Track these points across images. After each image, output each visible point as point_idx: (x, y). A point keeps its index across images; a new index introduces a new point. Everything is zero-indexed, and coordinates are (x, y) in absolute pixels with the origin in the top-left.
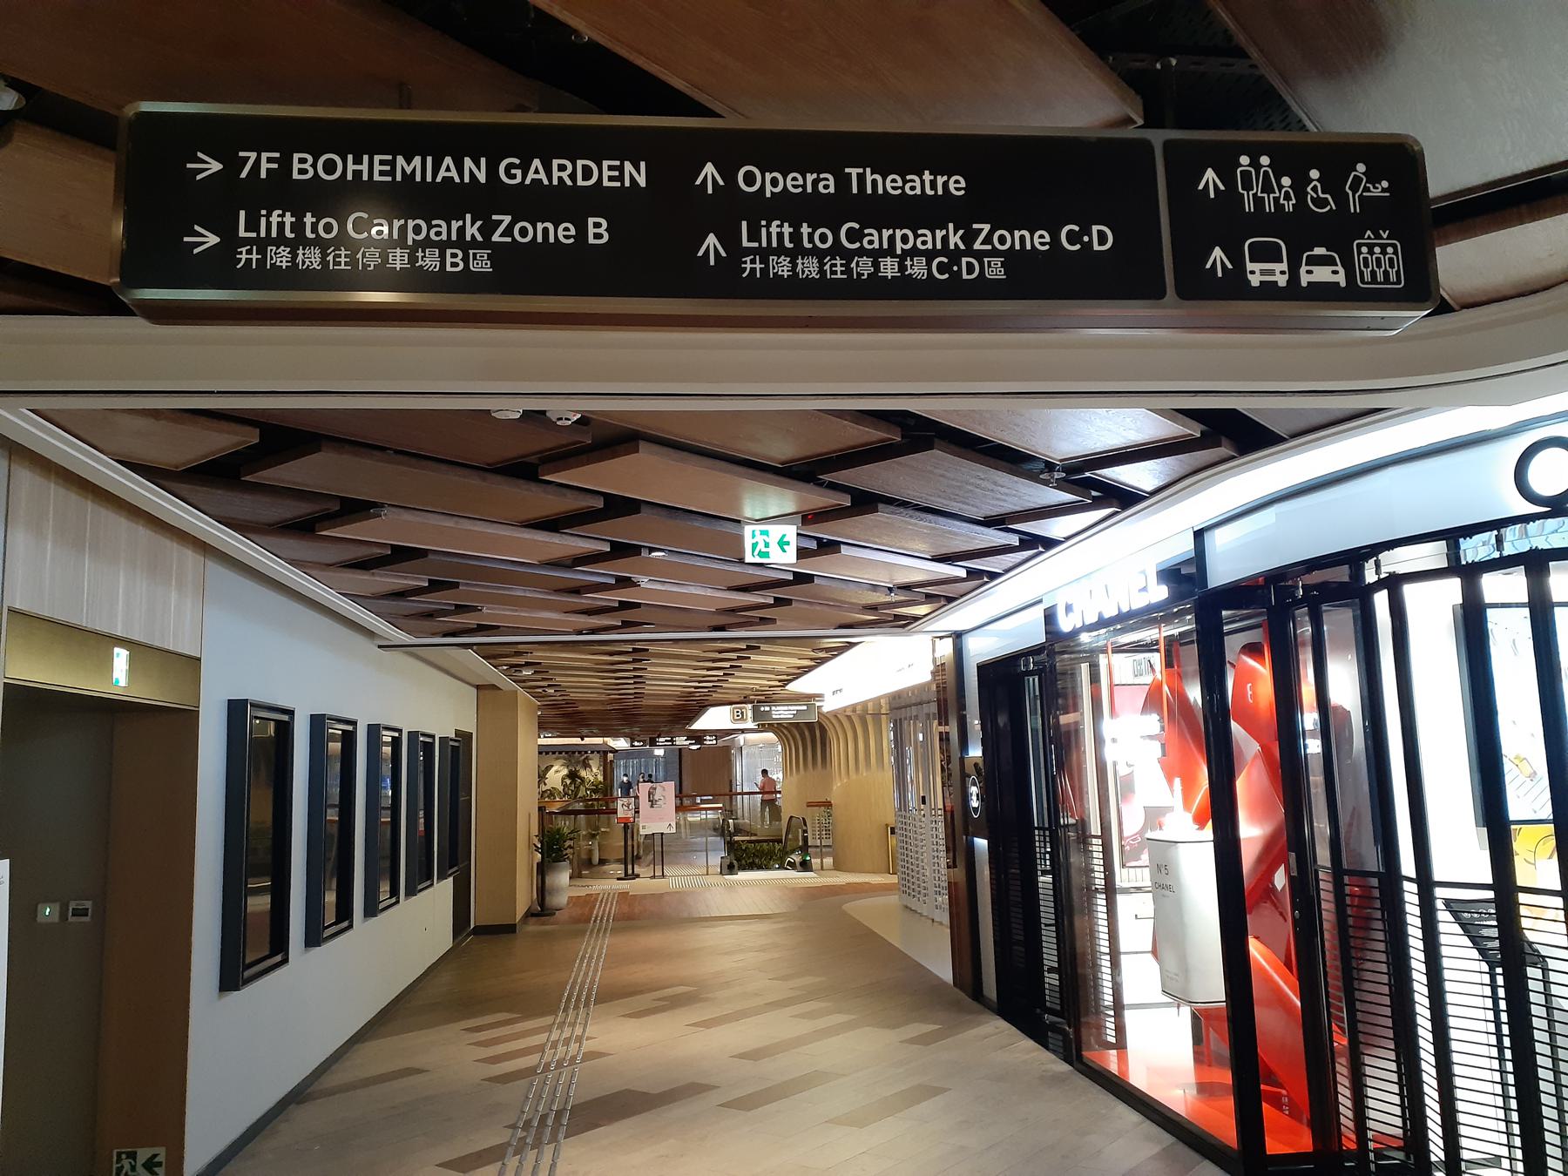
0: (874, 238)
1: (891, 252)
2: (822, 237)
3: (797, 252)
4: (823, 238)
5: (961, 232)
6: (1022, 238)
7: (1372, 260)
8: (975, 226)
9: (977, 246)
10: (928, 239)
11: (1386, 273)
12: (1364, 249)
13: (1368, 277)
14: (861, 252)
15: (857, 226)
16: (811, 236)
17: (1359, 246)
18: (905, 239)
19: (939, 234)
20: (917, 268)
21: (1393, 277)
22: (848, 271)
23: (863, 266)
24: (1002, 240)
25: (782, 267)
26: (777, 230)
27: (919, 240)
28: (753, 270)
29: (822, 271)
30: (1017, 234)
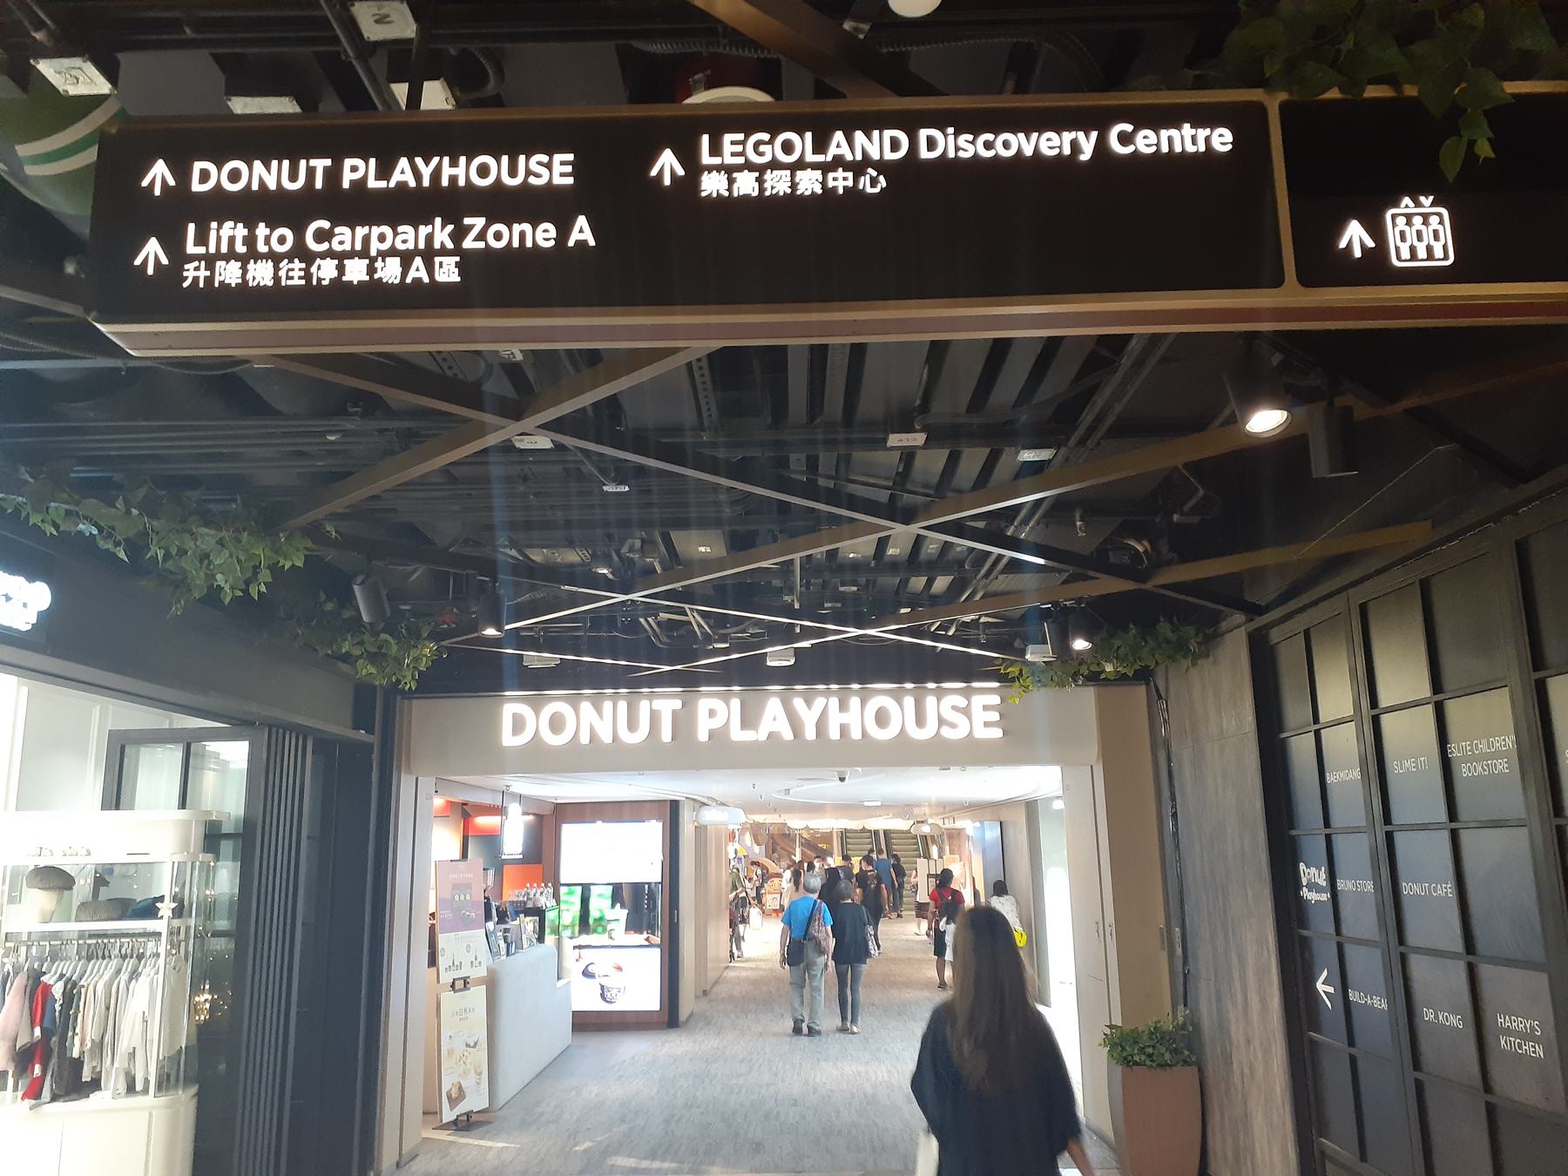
0: (344, 237)
2: (281, 238)
3: (253, 255)
4: (282, 240)
5: (450, 227)
6: (522, 235)
7: (1411, 236)
8: (467, 221)
9: (469, 243)
10: (408, 236)
11: (1429, 249)
13: (1406, 254)
15: (326, 224)
16: (267, 240)
17: (1394, 217)
18: (382, 238)
19: (424, 230)
21: (1439, 253)
23: (326, 271)
24: (498, 236)
25: (229, 273)
26: (232, 231)
27: (399, 238)
28: (196, 279)
29: (276, 278)
30: (517, 228)
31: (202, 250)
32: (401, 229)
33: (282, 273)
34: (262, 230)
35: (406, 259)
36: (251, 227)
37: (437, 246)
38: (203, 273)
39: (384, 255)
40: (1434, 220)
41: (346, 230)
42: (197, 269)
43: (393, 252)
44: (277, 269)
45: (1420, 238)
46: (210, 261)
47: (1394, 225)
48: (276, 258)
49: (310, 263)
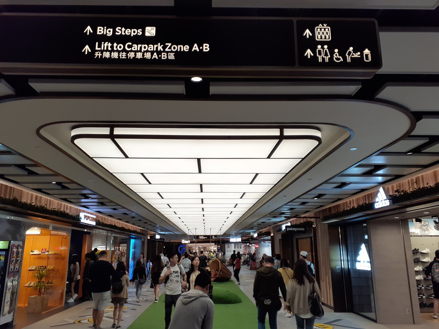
0: (135, 47)
1: (140, 51)
3: (112, 50)
4: (120, 47)
5: (162, 46)
6: (180, 48)
8: (167, 44)
10: (152, 47)
11: (325, 36)
12: (319, 29)
13: (319, 37)
14: (131, 51)
15: (130, 44)
17: (317, 29)
18: (145, 48)
19: (155, 46)
20: (148, 56)
22: (127, 56)
23: (131, 55)
24: (174, 48)
25: (107, 55)
26: (107, 45)
27: (149, 48)
28: (98, 56)
29: (119, 56)
30: (179, 46)
31: (100, 49)
32: (150, 45)
33: (120, 55)
34: (115, 45)
35: (152, 53)
36: (113, 44)
37: (159, 50)
38: (100, 55)
39: (144, 52)
40: (327, 30)
41: (136, 45)
42: (98, 53)
43: (147, 51)
44: (119, 54)
45: (323, 34)
46: (102, 52)
47: (317, 31)
48: (119, 52)
49: (127, 54)
